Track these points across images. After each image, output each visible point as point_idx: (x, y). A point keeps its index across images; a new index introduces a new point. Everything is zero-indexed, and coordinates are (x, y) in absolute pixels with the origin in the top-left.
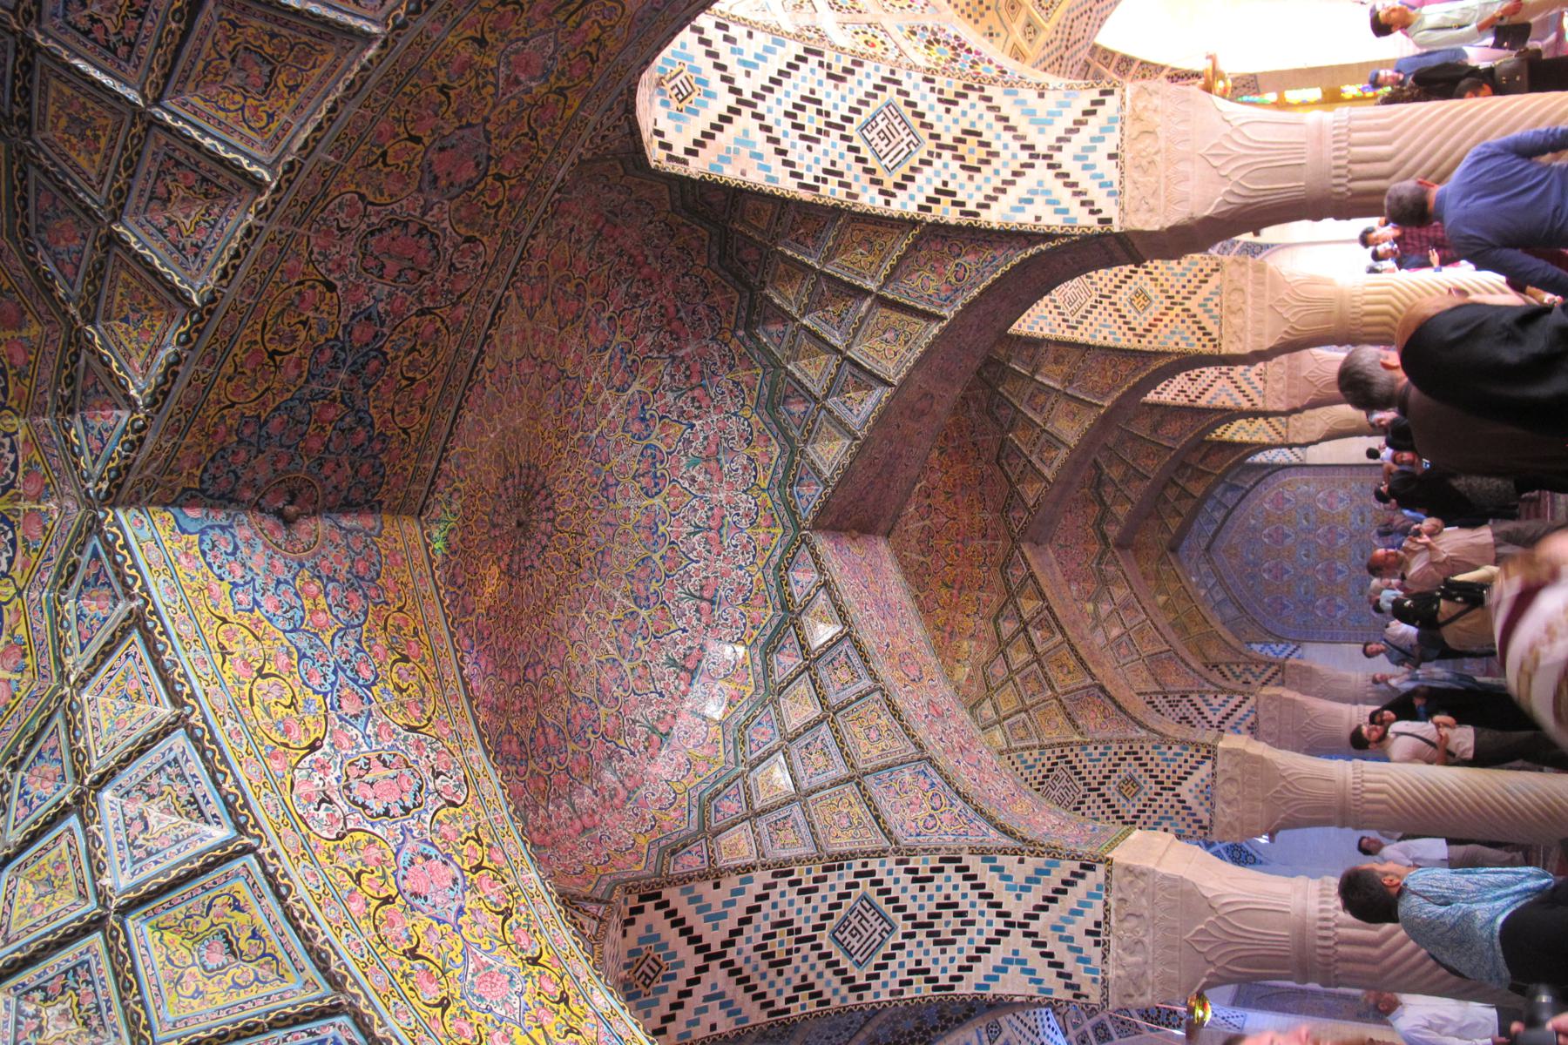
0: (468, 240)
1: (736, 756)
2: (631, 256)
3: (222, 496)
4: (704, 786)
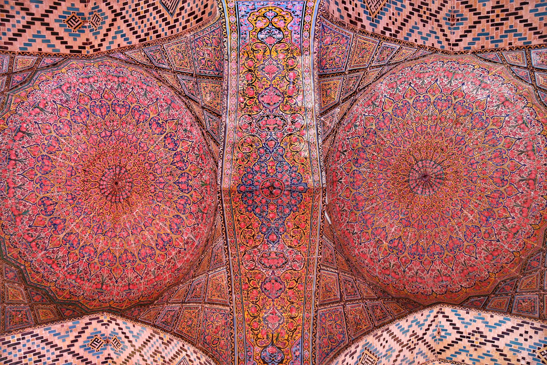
0: (253, 269)
1: (8, 98)
2: (84, 280)
4: (26, 87)
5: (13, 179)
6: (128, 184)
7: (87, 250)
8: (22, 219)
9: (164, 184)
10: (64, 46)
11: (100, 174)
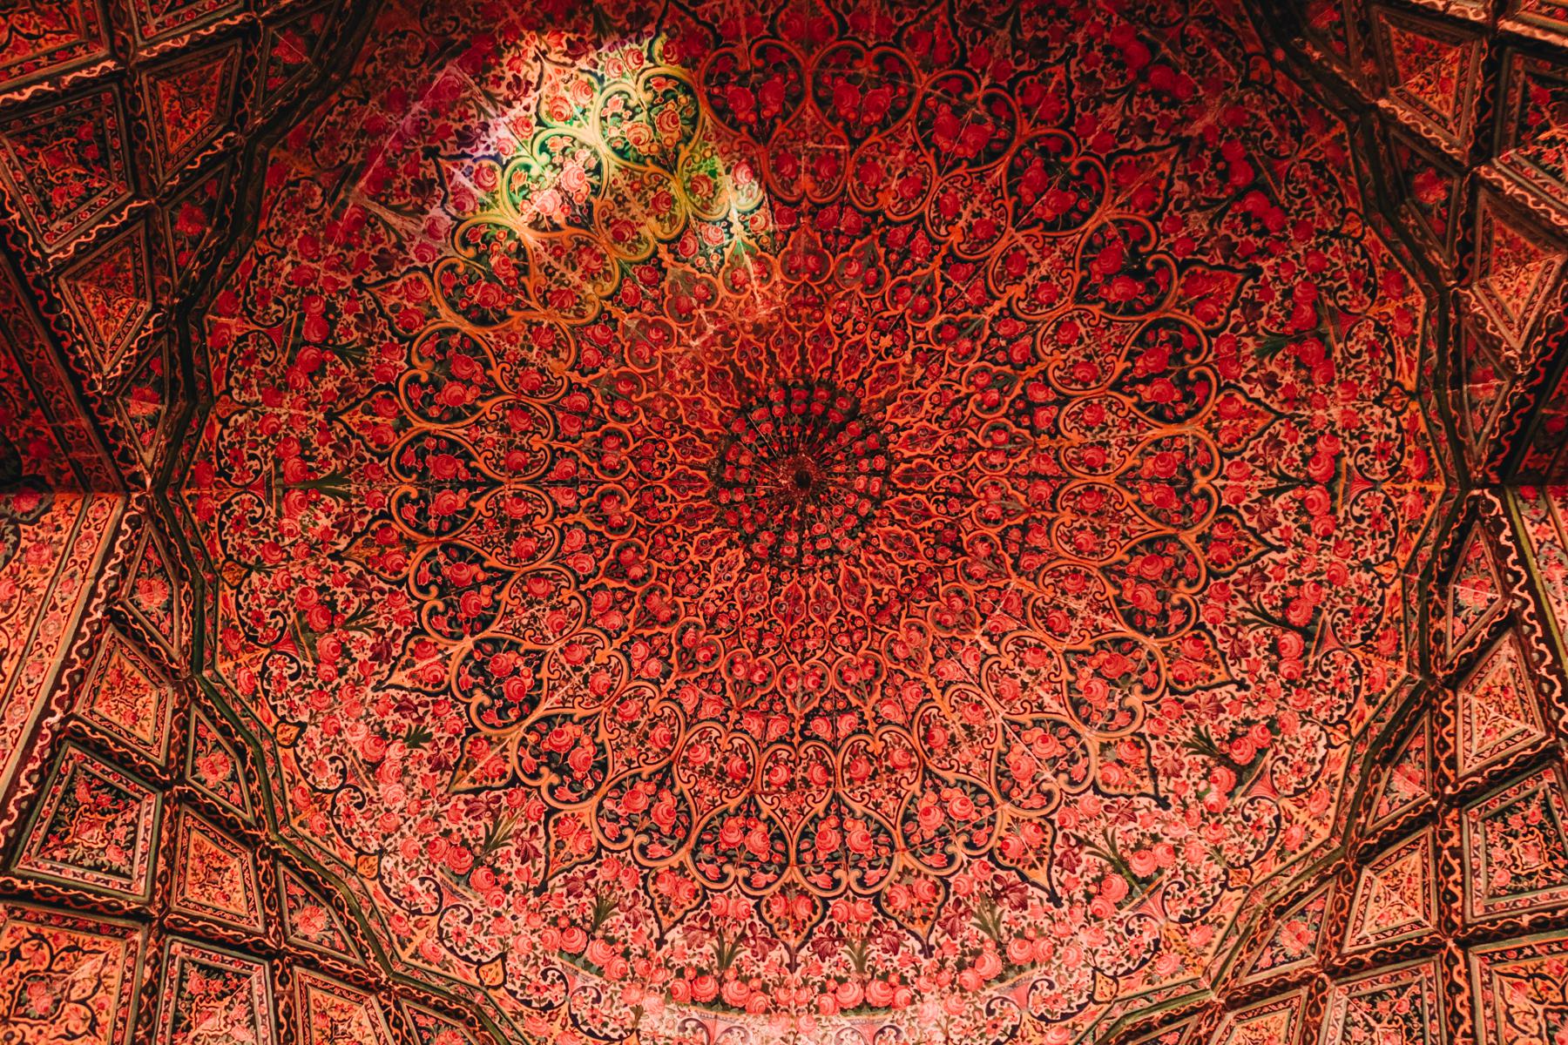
5: (1306, 529)
6: (742, 476)
7: (971, 139)
8: (1289, 315)
11: (881, 530)
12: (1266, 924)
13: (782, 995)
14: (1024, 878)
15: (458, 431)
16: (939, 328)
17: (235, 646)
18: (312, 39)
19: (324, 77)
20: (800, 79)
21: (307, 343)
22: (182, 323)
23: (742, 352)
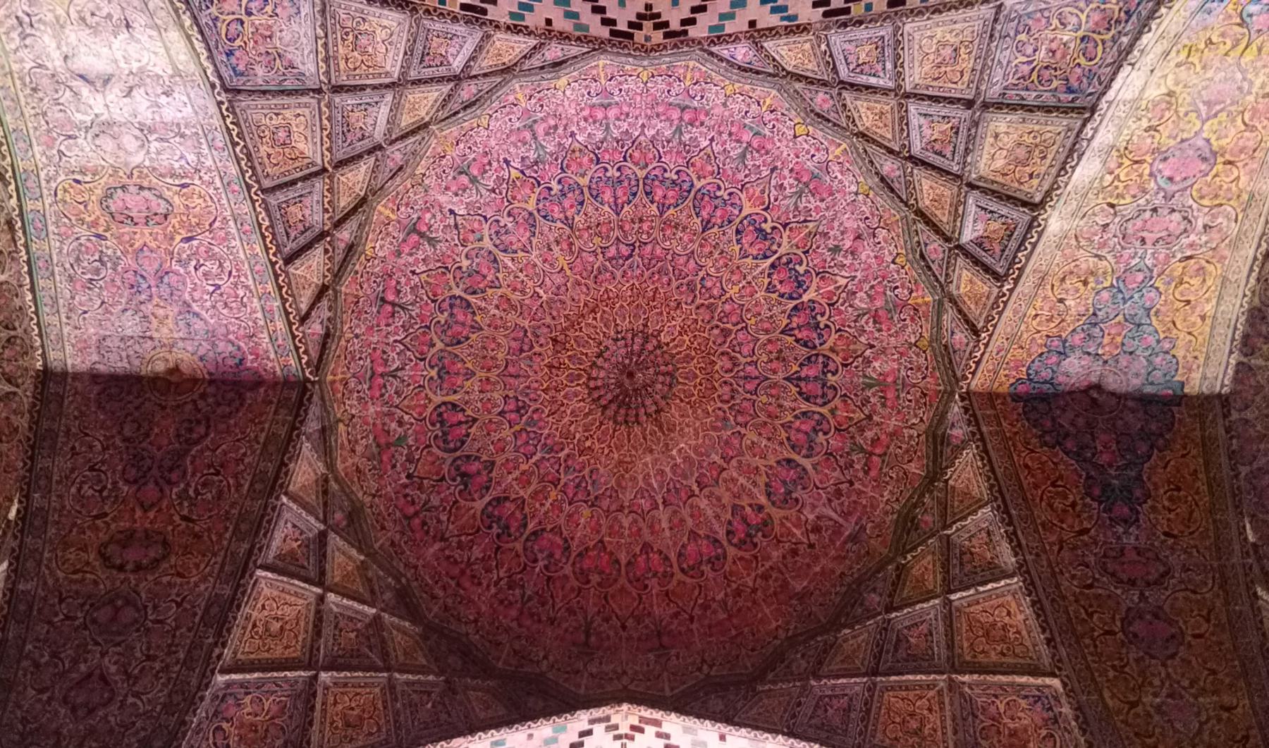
3: (1150, 402)
5: (384, 352)
6: (661, 378)
7: (545, 542)
9: (757, 381)
10: (598, 17)
12: (407, 162)
13: (649, 112)
14: (522, 172)
15: (804, 406)
16: (562, 449)
17: (924, 308)
18: (862, 604)
19: (860, 585)
20: (627, 573)
21: (880, 456)
22: (935, 474)
23: (659, 440)
